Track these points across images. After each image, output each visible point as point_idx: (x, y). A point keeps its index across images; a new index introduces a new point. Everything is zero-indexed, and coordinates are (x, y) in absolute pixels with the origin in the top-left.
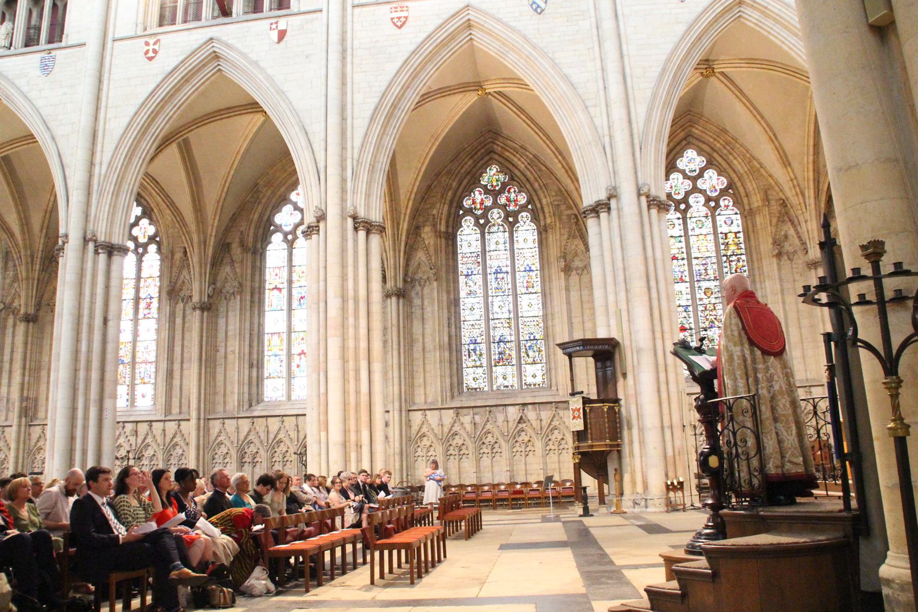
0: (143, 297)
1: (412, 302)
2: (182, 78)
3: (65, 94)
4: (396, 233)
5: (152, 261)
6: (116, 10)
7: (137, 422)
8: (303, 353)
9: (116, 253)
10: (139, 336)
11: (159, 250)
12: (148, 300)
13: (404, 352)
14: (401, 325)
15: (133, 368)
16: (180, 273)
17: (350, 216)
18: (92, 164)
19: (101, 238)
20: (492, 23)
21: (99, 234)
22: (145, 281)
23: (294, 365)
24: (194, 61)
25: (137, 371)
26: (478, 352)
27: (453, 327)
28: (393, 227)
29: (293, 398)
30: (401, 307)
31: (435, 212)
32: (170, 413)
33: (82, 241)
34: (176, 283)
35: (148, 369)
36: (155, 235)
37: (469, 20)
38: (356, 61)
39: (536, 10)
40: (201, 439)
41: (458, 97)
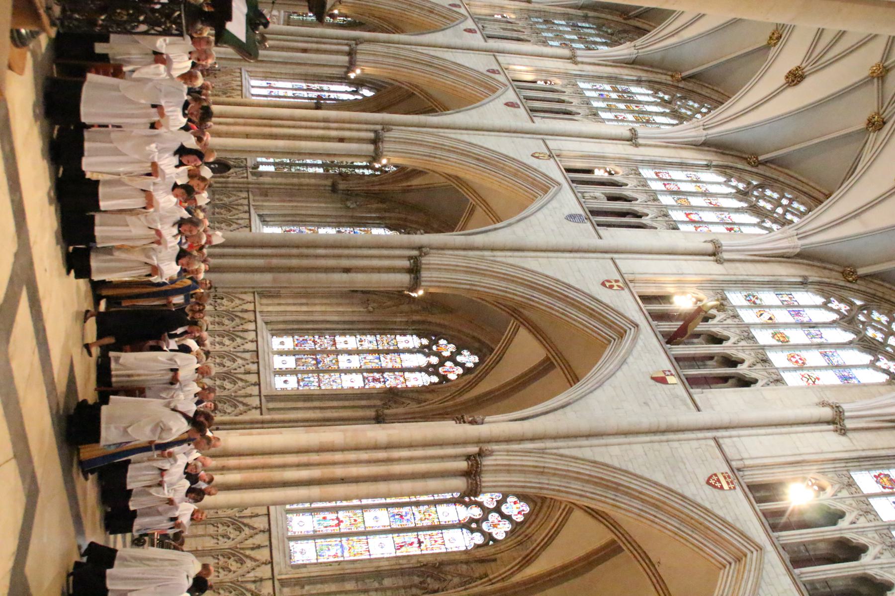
0: (385, 375)
3: (553, 230)
5: (422, 380)
6: (642, 259)
7: (258, 373)
8: (340, 522)
10: (346, 374)
11: (432, 384)
12: (382, 380)
15: (313, 372)
16: (413, 399)
17: (480, 449)
18: (493, 249)
19: (424, 260)
20: (751, 578)
21: (428, 258)
22: (401, 376)
23: (327, 515)
24: (612, 316)
25: (310, 375)
29: (289, 516)
32: (268, 401)
33: (419, 245)
35: (313, 384)
36: (448, 380)
37: (746, 556)
38: (656, 446)
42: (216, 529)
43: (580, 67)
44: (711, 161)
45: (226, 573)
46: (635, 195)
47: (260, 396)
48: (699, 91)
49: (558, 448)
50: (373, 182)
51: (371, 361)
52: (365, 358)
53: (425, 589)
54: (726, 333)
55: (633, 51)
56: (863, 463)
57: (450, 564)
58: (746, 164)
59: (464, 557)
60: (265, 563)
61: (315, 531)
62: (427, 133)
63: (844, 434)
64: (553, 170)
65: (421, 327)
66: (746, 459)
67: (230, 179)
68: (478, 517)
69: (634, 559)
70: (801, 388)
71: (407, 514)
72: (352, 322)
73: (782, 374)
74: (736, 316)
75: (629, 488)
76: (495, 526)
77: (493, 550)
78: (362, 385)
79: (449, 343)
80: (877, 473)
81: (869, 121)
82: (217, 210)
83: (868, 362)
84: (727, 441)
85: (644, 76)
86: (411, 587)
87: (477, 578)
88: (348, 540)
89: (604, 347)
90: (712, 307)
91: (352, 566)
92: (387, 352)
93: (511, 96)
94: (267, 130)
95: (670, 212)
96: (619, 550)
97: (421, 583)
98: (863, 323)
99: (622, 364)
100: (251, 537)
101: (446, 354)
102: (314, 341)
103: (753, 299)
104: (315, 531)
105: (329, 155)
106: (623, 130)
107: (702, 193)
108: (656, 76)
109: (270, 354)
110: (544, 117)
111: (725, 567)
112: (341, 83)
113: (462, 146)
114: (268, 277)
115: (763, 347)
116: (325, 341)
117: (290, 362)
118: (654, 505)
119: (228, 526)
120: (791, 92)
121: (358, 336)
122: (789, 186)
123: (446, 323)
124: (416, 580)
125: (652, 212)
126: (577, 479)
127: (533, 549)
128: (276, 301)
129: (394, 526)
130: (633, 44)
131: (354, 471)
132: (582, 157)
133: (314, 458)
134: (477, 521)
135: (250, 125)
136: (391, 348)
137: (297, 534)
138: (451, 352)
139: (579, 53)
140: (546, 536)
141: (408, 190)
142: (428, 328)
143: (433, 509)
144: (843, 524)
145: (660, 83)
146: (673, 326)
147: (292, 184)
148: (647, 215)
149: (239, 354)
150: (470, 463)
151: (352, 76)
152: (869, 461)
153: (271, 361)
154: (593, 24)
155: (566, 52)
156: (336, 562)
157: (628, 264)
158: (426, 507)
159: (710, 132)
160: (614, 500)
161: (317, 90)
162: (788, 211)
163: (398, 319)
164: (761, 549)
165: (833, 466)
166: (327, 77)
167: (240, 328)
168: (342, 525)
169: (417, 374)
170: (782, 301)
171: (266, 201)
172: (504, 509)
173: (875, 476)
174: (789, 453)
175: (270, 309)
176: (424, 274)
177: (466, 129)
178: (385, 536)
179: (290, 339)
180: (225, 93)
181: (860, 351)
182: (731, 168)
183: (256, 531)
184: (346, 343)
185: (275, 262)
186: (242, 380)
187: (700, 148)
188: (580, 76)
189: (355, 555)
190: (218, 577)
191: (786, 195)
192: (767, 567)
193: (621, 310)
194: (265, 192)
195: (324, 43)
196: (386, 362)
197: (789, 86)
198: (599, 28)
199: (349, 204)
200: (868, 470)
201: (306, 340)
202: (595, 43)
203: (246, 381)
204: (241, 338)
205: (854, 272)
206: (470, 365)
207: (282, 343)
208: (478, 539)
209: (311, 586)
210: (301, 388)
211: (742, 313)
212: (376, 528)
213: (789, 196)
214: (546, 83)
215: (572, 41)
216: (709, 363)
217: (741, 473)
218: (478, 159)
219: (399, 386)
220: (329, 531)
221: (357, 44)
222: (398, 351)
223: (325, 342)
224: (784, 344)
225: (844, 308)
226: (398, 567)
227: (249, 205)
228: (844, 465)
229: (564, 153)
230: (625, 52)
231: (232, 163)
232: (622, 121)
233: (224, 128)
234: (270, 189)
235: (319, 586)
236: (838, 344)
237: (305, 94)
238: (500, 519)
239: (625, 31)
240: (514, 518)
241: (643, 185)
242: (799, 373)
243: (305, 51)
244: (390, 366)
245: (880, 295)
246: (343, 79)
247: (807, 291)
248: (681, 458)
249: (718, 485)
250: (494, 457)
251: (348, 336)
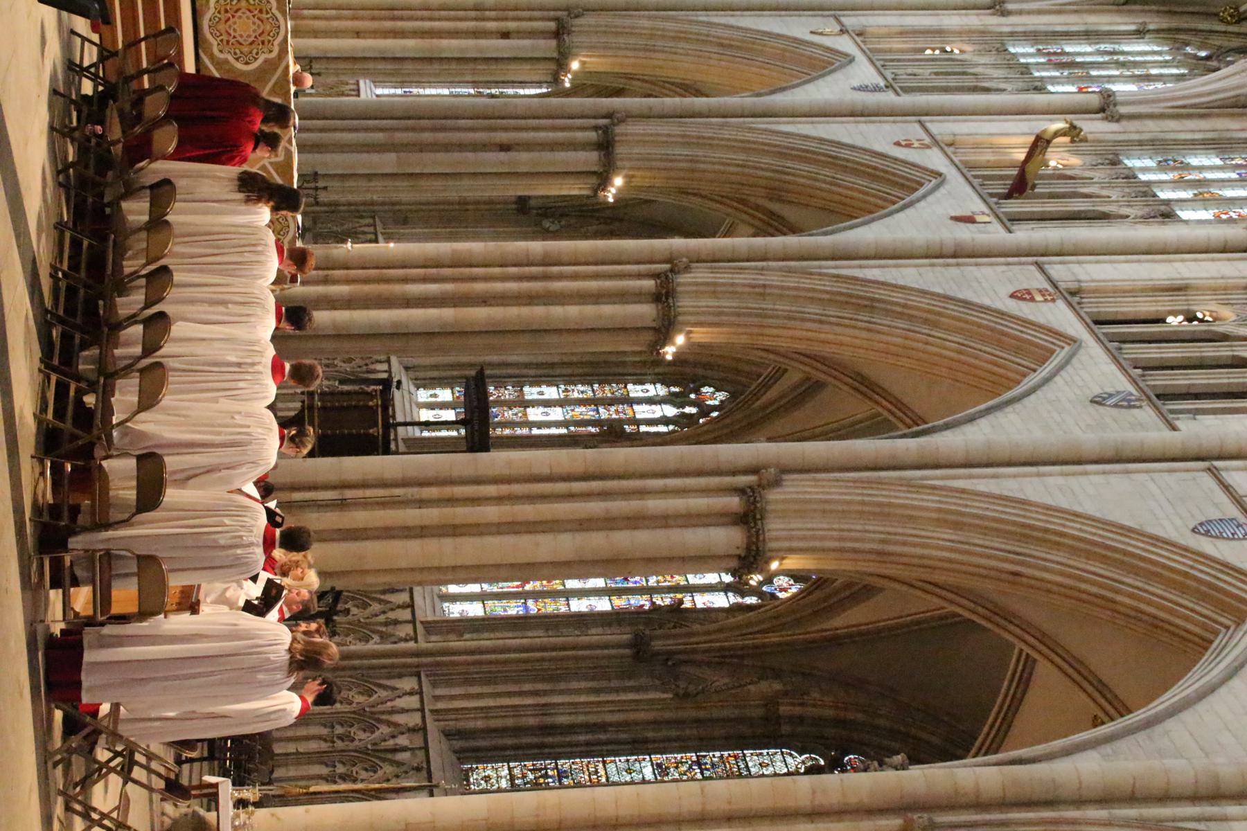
9: (603, 153)
19: (619, 129)
26: (541, 780)
27: (589, 737)
31: (816, 695)
79: (718, 390)
109: (414, 406)
118: (926, 321)
121: (562, 386)
131: (499, 286)
150: (659, 281)
160: (869, 322)
176: (620, 150)
185: (400, 137)
218: (722, 45)
238: (792, 582)
249: (1028, 297)
250: (692, 275)
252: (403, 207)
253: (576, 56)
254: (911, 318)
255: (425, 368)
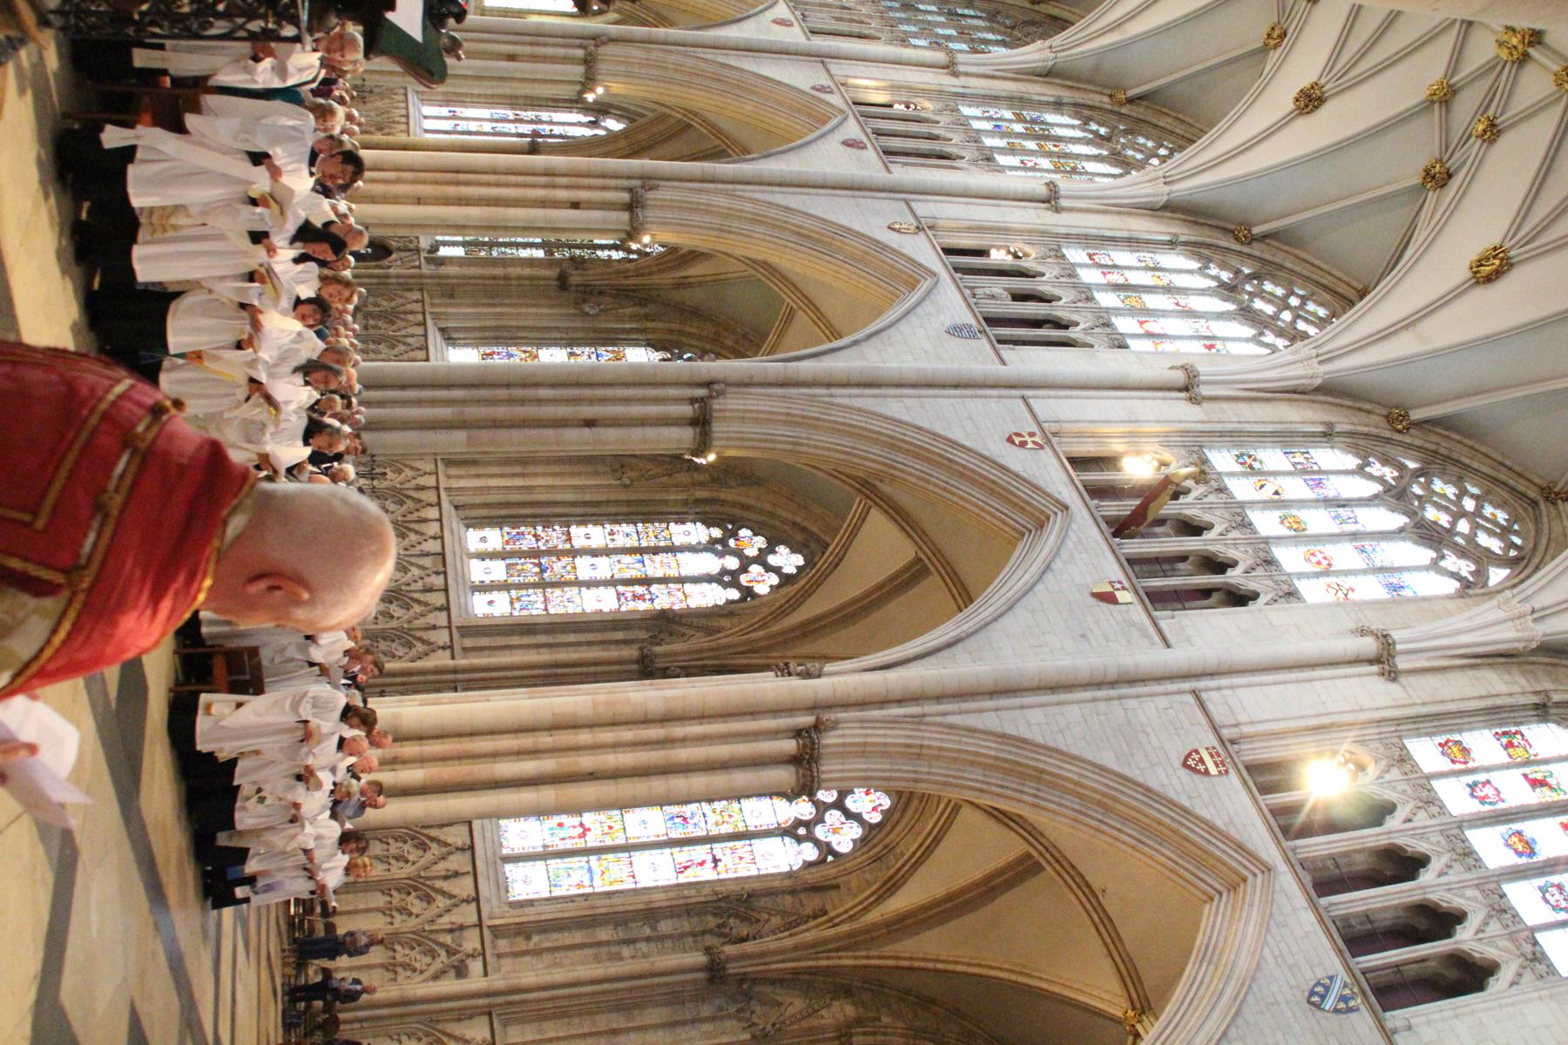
1: (703, 1000)
2: (993, 482)
3: (926, 352)
4: (830, 946)
5: (714, 596)
6: (1071, 397)
7: (446, 590)
8: (586, 830)
9: (698, 430)
11: (730, 602)
12: (648, 597)
13: (603, 992)
14: (656, 980)
15: (534, 585)
16: (699, 628)
17: (818, 718)
18: (829, 385)
19: (716, 405)
21: (721, 401)
23: (564, 818)
24: (1025, 492)
25: (531, 591)
28: (837, 938)
29: (503, 822)
30: (689, 976)
31: (886, 1020)
32: (463, 636)
33: (709, 379)
34: (680, 624)
37: (1245, 880)
38: (1102, 706)
39: (1312, 993)
40: (422, 678)
41: (1114, 985)
42: (385, 846)
43: (962, 81)
44: (1176, 235)
45: (405, 917)
46: (1056, 292)
47: (450, 627)
48: (1154, 121)
49: (944, 714)
50: (627, 271)
51: (629, 567)
52: (619, 561)
53: (726, 935)
54: (1207, 517)
55: (1047, 54)
56: (1421, 725)
57: (765, 896)
58: (1233, 240)
59: (787, 883)
60: (467, 901)
61: (545, 846)
62: (717, 192)
63: (1394, 680)
64: (923, 251)
65: (708, 509)
66: (1246, 724)
67: (392, 271)
68: (807, 817)
69: (1066, 890)
70: (1327, 605)
71: (693, 815)
72: (598, 503)
73: (1296, 582)
74: (1222, 490)
75: (1058, 776)
76: (835, 831)
77: (834, 871)
78: (614, 605)
79: (755, 534)
80: (1442, 739)
81: (1427, 172)
82: (371, 322)
83: (1427, 562)
84: (1214, 695)
85: (1067, 95)
86: (703, 933)
87: (809, 917)
88: (599, 859)
89: (1013, 545)
90: (1187, 477)
91: (607, 902)
92: (656, 551)
93: (852, 129)
94: (452, 190)
95: (1114, 320)
96: (1037, 869)
97: (719, 926)
98: (1419, 498)
99: (1044, 573)
100: (443, 858)
101: (751, 552)
102: (535, 536)
103: (1249, 461)
104: (545, 846)
105: (555, 230)
106: (1035, 184)
107: (1163, 288)
108: (1084, 95)
110: (906, 164)
111: (1212, 899)
112: (569, 109)
113: (773, 213)
114: (460, 436)
115: (1267, 541)
116: (554, 534)
117: (498, 571)
118: (1099, 803)
119: (405, 842)
120: (1302, 123)
121: (607, 526)
122: (1300, 275)
123: (751, 502)
124: (712, 922)
125: (1084, 320)
126: (972, 763)
127: (899, 870)
128: (473, 470)
129: (674, 835)
130: (1048, 43)
131: (612, 760)
132: (969, 229)
133: (545, 740)
134: (808, 825)
135: (424, 182)
136: (662, 544)
137: (516, 851)
138: (760, 550)
139: (960, 57)
140: (920, 846)
141: (681, 285)
142: (721, 509)
143: (735, 805)
144: (1393, 822)
145: (1091, 108)
146: (1125, 507)
147: (494, 278)
148: (1077, 324)
149: (413, 560)
151: (590, 97)
152: (1432, 721)
153: (466, 570)
154: (983, 11)
155: (939, 56)
156: (582, 895)
157: (1051, 407)
158: (724, 803)
159: (1175, 187)
161: (532, 122)
162: (1299, 316)
163: (673, 497)
164: (1269, 870)
165: (1377, 730)
166: (547, 99)
167: (415, 516)
168: (589, 836)
169: (705, 587)
170: (1294, 464)
171: (451, 305)
172: (849, 803)
173: (1440, 744)
174: (1313, 712)
175: (463, 483)
176: (717, 428)
177: (780, 185)
178: (658, 851)
179: (497, 532)
180: (380, 129)
181: (1415, 543)
182: (1209, 246)
183: (450, 850)
184: (588, 537)
185: (473, 412)
186: (419, 602)
187: (1159, 213)
188: (963, 95)
189: (611, 884)
190: (392, 924)
191: (1297, 291)
192: (1280, 898)
193: (1041, 484)
194: (449, 290)
195: (545, 45)
196: (656, 566)
197: (1301, 114)
198: (992, 17)
199: (587, 308)
200: (1430, 735)
201: (523, 534)
202: (987, 42)
203: (426, 604)
204: (416, 532)
205: (1405, 416)
206: (790, 569)
207: (484, 540)
208: (810, 852)
209: (543, 936)
210: (516, 613)
211: (1231, 484)
212: (644, 840)
213: (1301, 292)
214: (908, 107)
215: (949, 38)
216: (1181, 566)
217: (1236, 747)
218: (799, 234)
219: (676, 607)
220: (568, 845)
221: (597, 46)
222: (672, 549)
223: (554, 536)
224: (1299, 536)
225: (1389, 473)
226: (681, 902)
227: (424, 314)
228: (1393, 729)
229: (942, 223)
230: (1036, 56)
231: (394, 244)
232: (1033, 169)
233: (379, 189)
234: (458, 285)
235: (555, 936)
236: (1381, 533)
237: (511, 128)
238: (843, 819)
239: (1033, 23)
240: (866, 817)
241: (1070, 276)
242: (1323, 580)
243: (512, 57)
244: (659, 574)
245: (1445, 452)
246: (576, 103)
247: (1332, 447)
248: (1142, 725)
249: (1200, 767)
251: (590, 526)
252: (450, 281)
253: (645, 231)
254: (1082, 797)
255: (474, 506)
